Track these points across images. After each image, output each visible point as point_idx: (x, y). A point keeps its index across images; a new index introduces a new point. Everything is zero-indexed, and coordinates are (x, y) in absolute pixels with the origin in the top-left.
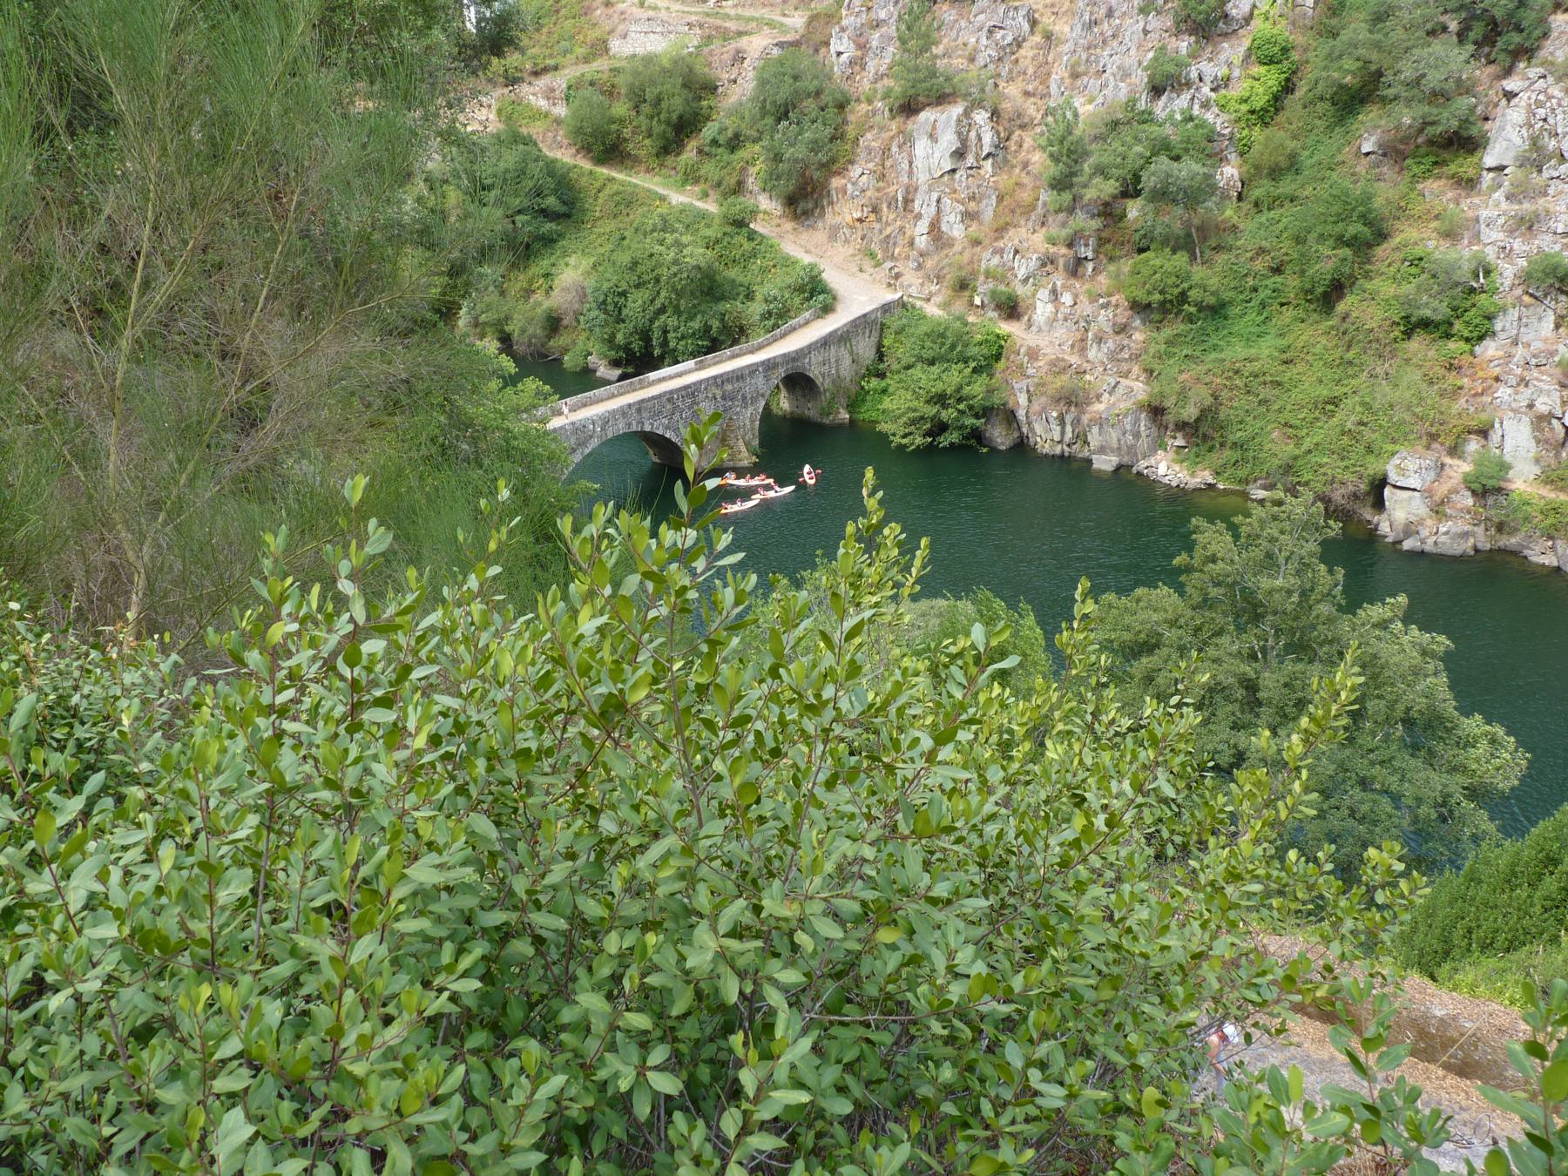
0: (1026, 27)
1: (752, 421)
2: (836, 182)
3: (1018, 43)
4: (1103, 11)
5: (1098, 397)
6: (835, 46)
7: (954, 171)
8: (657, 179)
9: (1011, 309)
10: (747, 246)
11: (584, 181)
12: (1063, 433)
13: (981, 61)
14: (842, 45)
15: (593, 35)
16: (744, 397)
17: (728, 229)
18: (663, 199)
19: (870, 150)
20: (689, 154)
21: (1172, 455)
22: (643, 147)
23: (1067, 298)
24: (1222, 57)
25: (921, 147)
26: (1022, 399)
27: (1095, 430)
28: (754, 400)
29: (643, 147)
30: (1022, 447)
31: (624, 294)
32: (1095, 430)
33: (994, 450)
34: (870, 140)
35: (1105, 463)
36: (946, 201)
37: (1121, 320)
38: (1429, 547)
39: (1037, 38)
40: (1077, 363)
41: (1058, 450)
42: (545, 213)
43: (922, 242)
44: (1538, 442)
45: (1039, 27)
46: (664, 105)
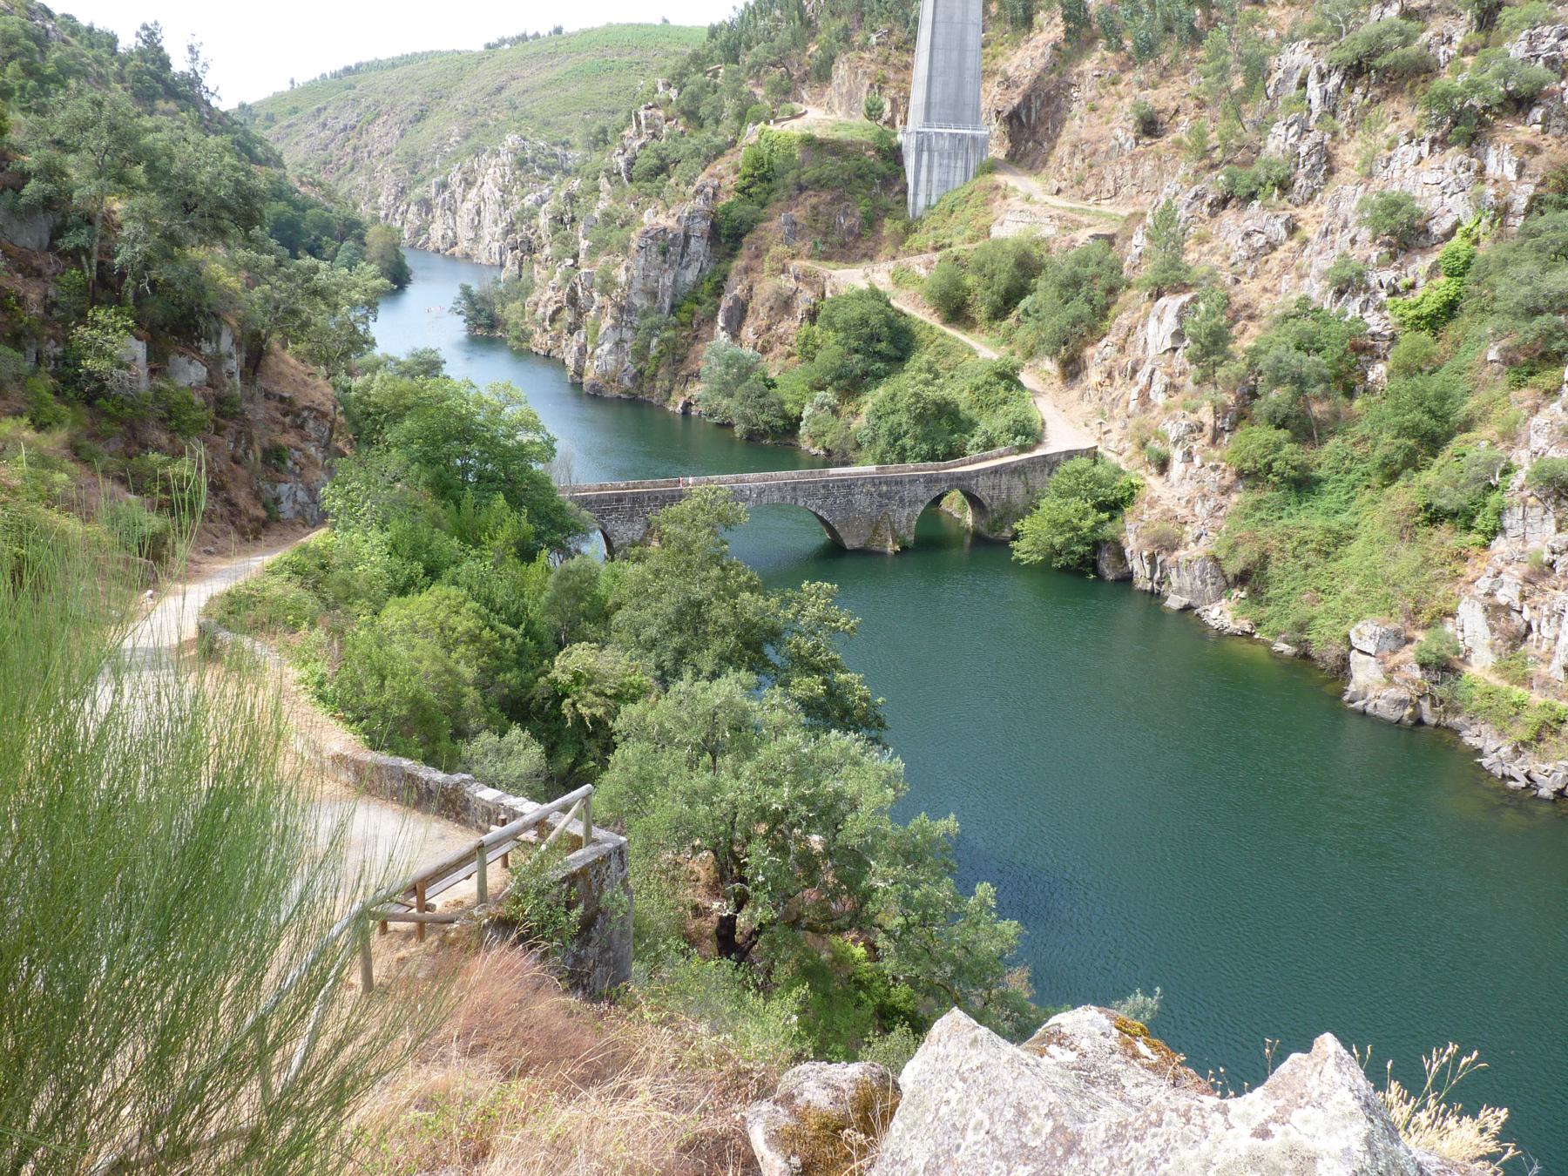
0: (1283, 233)
1: (909, 521)
2: (1089, 351)
3: (1272, 247)
4: (1340, 223)
5: (1186, 545)
6: (1135, 241)
7: (1175, 349)
8: (985, 338)
9: (1163, 465)
10: (1002, 394)
11: (923, 335)
12: (1153, 572)
13: (1232, 261)
14: (1139, 241)
15: (982, 221)
16: (902, 500)
17: (993, 379)
18: (972, 352)
19: (1120, 326)
20: (1011, 320)
21: (1232, 604)
22: (981, 312)
23: (1197, 461)
24: (1411, 269)
25: (1152, 322)
26: (1131, 538)
27: (1174, 572)
28: (912, 503)
29: (981, 312)
30: (1127, 579)
31: (880, 418)
32: (1174, 572)
33: (1100, 578)
34: (1125, 320)
35: (1174, 602)
36: (1158, 373)
37: (1226, 483)
38: (1369, 709)
39: (1294, 243)
40: (1185, 514)
41: (1149, 587)
42: (880, 356)
43: (1133, 405)
44: (1493, 630)
45: (1298, 235)
46: (996, 279)
